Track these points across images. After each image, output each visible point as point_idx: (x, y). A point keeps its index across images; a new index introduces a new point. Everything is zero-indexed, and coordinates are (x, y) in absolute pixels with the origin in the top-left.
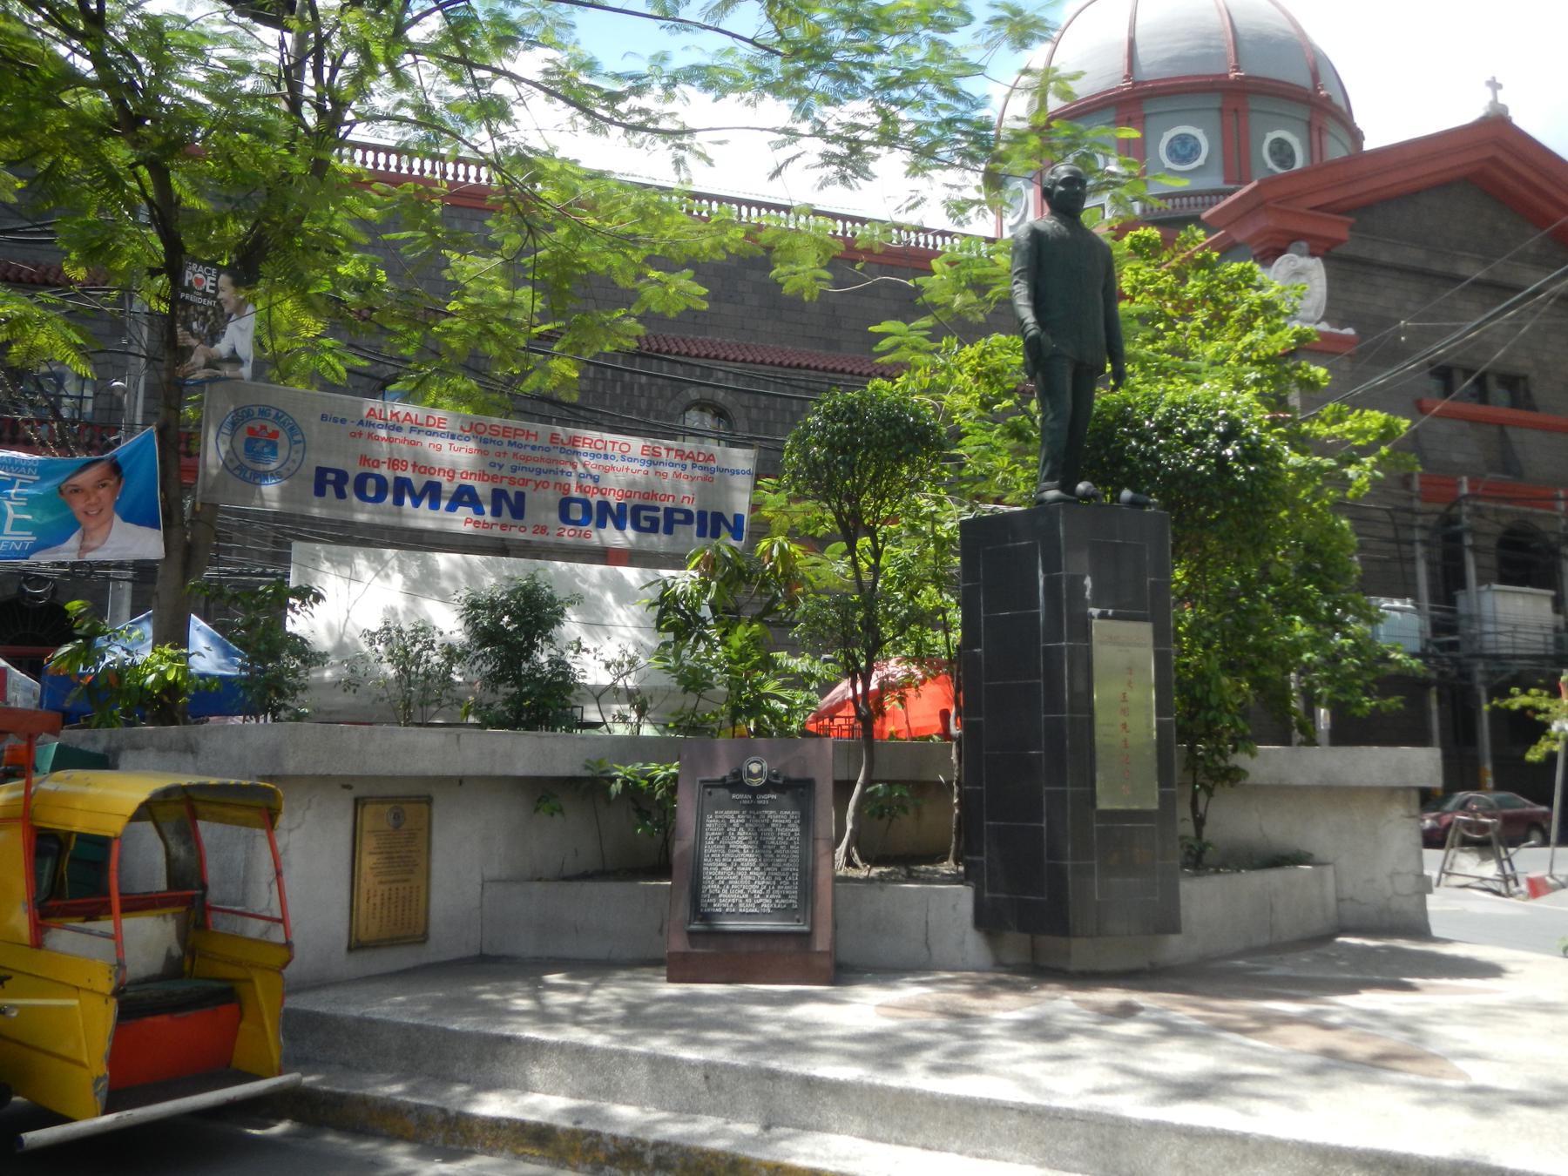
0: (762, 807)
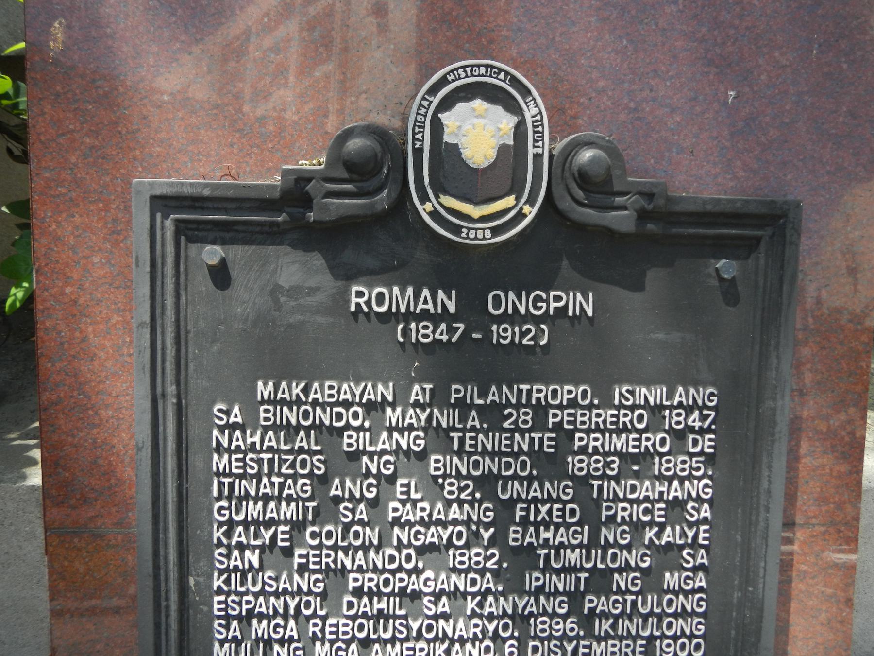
0: (519, 364)
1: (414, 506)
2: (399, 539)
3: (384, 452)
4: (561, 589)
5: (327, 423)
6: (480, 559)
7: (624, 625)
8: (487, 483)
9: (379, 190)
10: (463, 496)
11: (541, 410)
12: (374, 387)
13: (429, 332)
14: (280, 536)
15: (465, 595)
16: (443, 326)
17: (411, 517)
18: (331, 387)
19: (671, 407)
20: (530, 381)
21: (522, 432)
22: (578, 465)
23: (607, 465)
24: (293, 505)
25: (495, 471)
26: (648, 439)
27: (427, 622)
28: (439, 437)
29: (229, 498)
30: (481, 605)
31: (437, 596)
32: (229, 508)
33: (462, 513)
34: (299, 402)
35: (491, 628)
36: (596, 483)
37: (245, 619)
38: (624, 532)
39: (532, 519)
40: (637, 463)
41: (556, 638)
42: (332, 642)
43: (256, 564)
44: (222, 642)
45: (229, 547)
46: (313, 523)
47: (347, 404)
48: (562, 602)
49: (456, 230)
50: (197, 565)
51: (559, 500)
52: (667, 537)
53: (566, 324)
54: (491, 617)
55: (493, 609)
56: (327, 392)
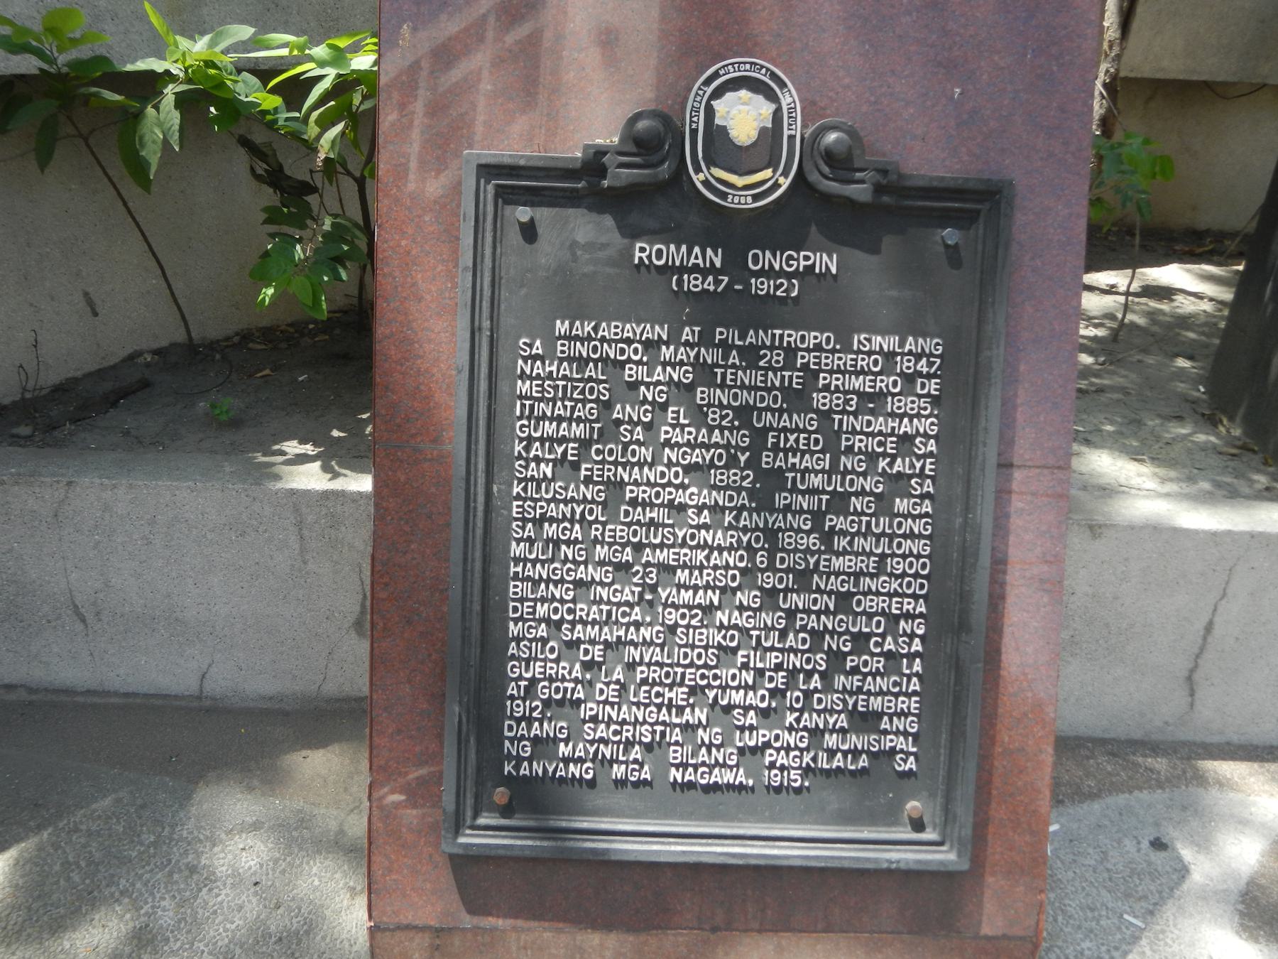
1: (682, 431)
2: (669, 458)
3: (658, 383)
4: (805, 507)
5: (612, 356)
6: (737, 478)
7: (859, 542)
8: (744, 413)
9: (662, 162)
10: (724, 423)
11: (791, 352)
12: (653, 328)
13: (699, 282)
14: (570, 452)
15: (723, 509)
16: (710, 278)
17: (679, 439)
18: (616, 327)
19: (903, 354)
20: (783, 327)
21: (775, 370)
22: (822, 401)
23: (847, 402)
24: (582, 425)
25: (751, 402)
26: (882, 381)
27: (691, 531)
28: (704, 373)
29: (529, 418)
30: (737, 518)
31: (700, 509)
32: (529, 426)
33: (723, 438)
34: (589, 338)
35: (745, 539)
36: (837, 417)
37: (539, 522)
38: (860, 461)
39: (782, 445)
40: (873, 401)
41: (800, 551)
42: (610, 545)
43: (549, 475)
44: (518, 541)
45: (527, 460)
46: (597, 442)
47: (629, 341)
48: (806, 519)
49: (724, 196)
50: (500, 475)
51: (805, 431)
52: (898, 466)
53: (814, 280)
54: (745, 530)
55: (747, 523)
56: (613, 330)
